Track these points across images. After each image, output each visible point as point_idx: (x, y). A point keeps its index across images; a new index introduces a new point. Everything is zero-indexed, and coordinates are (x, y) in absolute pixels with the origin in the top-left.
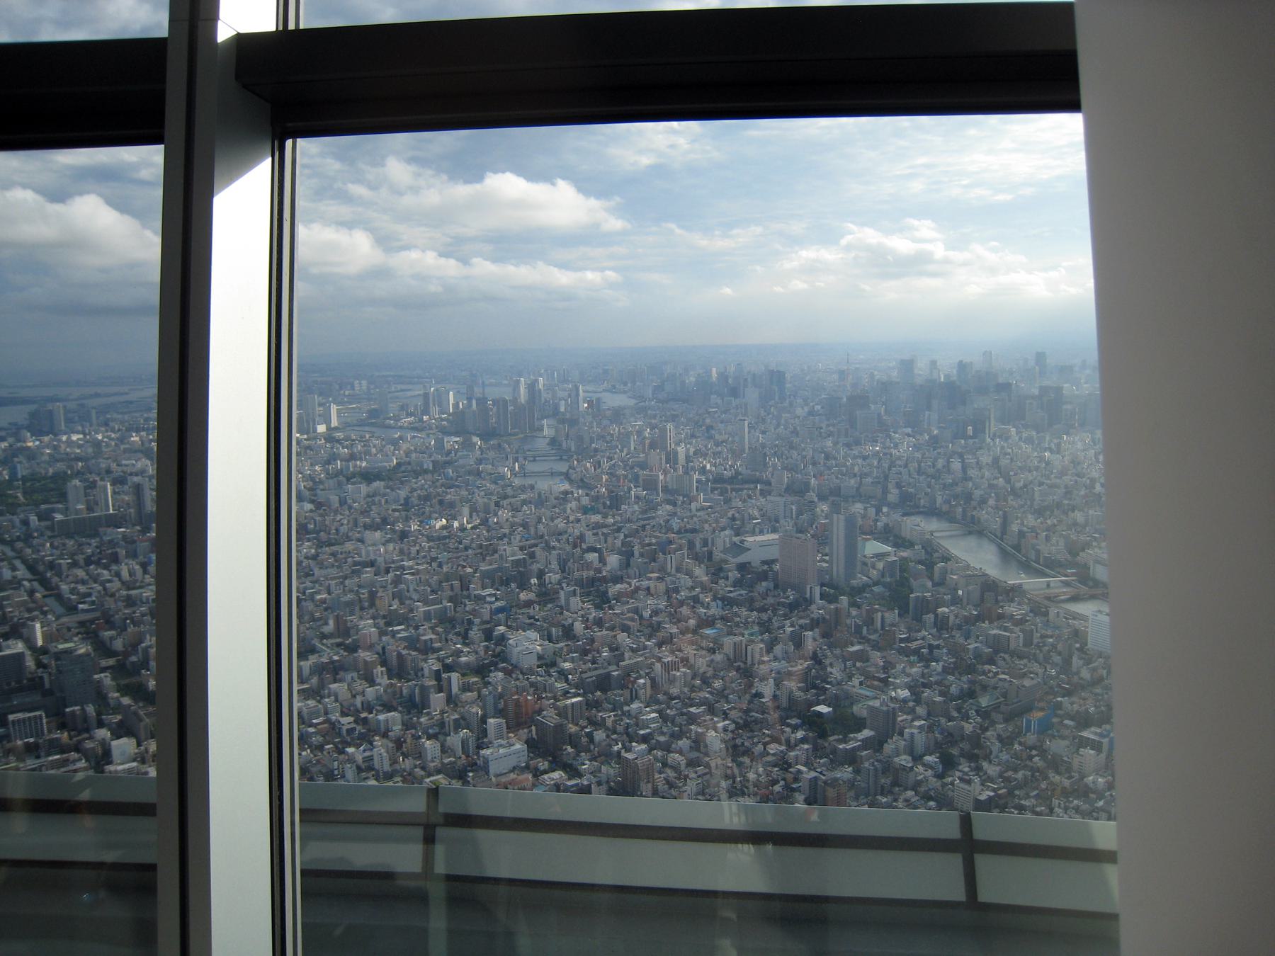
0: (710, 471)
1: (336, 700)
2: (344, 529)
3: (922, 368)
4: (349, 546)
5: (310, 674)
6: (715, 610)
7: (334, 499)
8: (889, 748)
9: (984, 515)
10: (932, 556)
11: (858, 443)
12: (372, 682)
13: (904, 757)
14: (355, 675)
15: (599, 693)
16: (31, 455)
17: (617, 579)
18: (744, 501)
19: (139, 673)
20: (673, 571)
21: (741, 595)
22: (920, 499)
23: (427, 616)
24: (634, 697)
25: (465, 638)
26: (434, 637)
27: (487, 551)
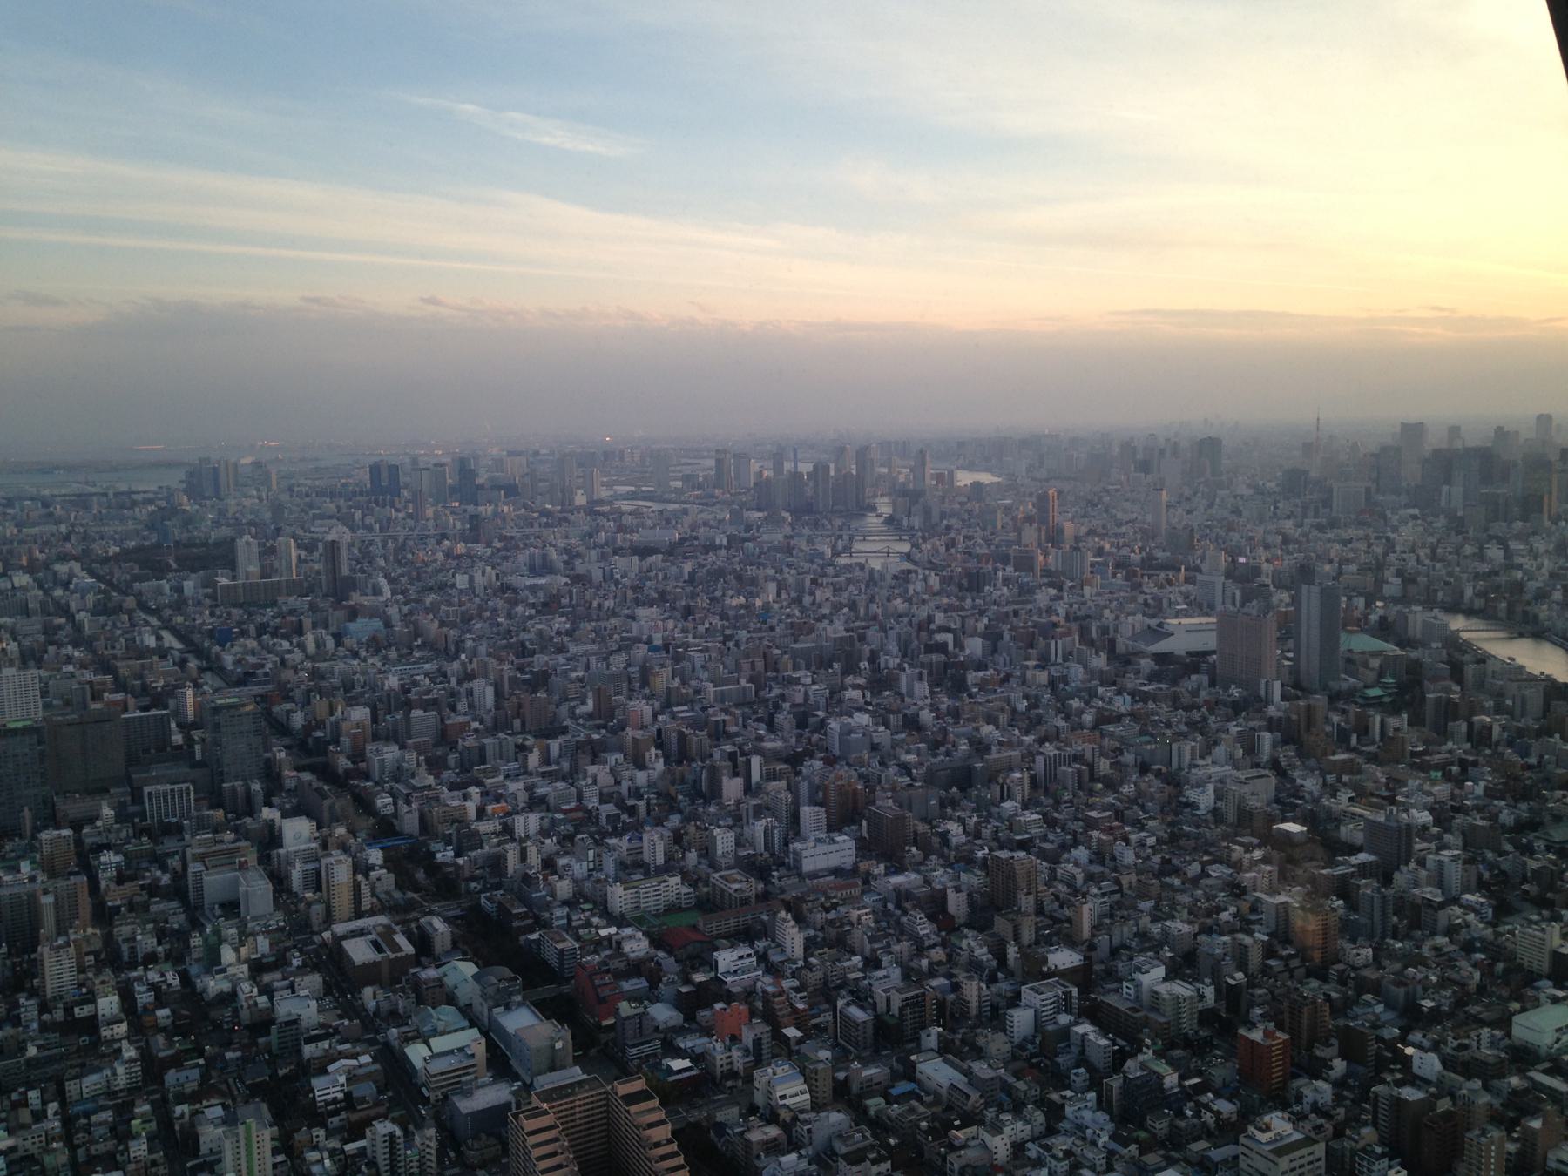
0: (1109, 554)
1: (595, 782)
2: (609, 604)
3: (1435, 440)
4: (614, 622)
5: (560, 756)
6: (1122, 704)
7: (597, 575)
8: (1400, 879)
9: (1543, 612)
10: (1458, 657)
11: (1333, 524)
12: (641, 765)
13: (1429, 889)
14: (620, 757)
15: (955, 789)
16: (188, 521)
17: (981, 666)
18: (1161, 587)
19: (325, 752)
20: (1060, 660)
21: (1161, 689)
22: (1436, 591)
23: (721, 698)
24: (1006, 795)
25: (771, 726)
26: (727, 718)
27: (797, 631)
